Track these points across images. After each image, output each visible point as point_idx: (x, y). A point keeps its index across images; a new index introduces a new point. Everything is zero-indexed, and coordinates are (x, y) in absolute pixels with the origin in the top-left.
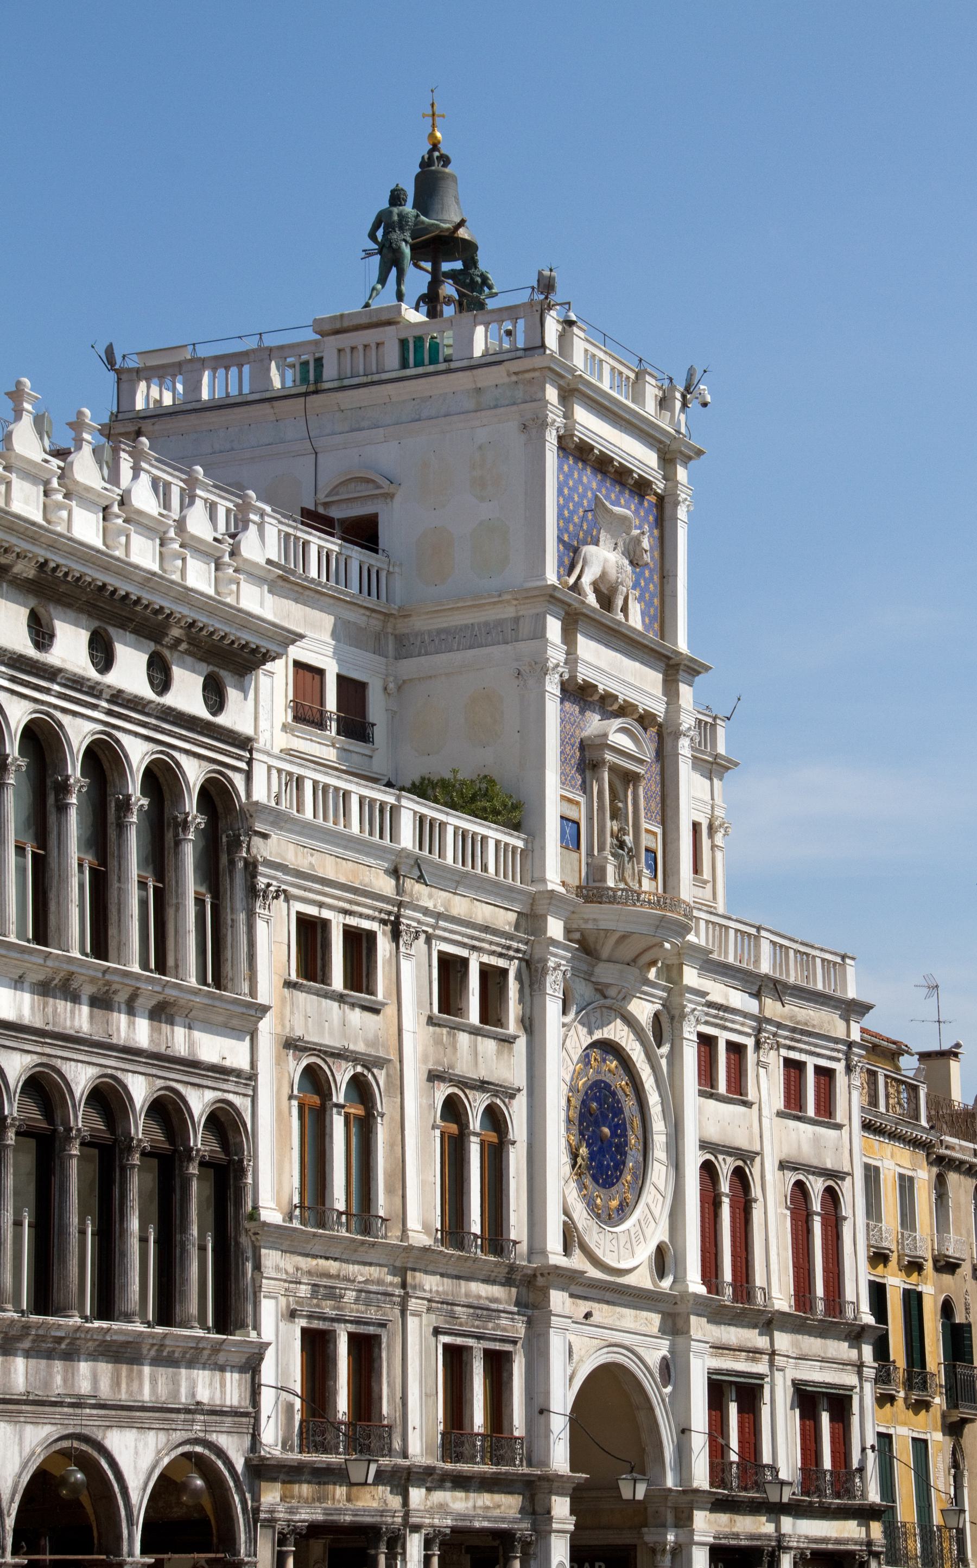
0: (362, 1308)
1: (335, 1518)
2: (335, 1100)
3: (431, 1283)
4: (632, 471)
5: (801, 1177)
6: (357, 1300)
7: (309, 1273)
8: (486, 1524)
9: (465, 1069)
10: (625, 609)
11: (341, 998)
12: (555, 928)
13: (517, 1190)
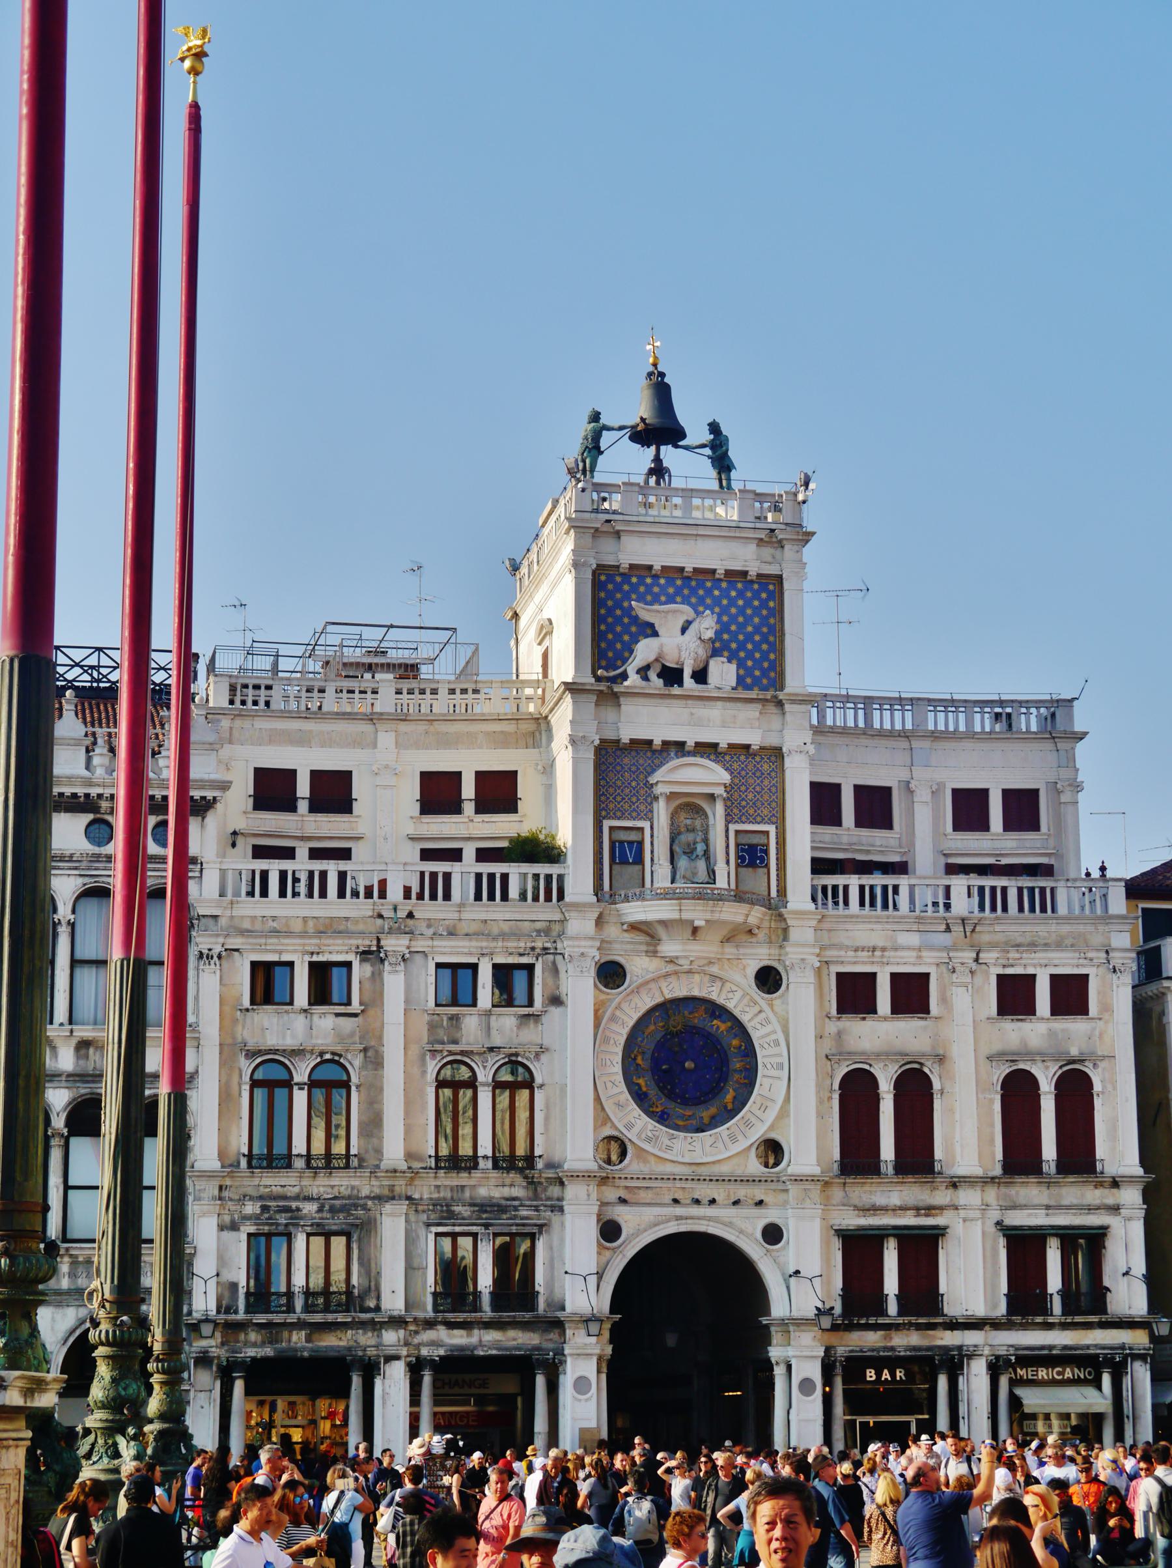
1: (290, 1354)
5: (1021, 1066)
6: (320, 1210)
7: (261, 1198)
8: (494, 1352)
9: (472, 1039)
10: (701, 676)
12: (581, 925)
13: (547, 1119)
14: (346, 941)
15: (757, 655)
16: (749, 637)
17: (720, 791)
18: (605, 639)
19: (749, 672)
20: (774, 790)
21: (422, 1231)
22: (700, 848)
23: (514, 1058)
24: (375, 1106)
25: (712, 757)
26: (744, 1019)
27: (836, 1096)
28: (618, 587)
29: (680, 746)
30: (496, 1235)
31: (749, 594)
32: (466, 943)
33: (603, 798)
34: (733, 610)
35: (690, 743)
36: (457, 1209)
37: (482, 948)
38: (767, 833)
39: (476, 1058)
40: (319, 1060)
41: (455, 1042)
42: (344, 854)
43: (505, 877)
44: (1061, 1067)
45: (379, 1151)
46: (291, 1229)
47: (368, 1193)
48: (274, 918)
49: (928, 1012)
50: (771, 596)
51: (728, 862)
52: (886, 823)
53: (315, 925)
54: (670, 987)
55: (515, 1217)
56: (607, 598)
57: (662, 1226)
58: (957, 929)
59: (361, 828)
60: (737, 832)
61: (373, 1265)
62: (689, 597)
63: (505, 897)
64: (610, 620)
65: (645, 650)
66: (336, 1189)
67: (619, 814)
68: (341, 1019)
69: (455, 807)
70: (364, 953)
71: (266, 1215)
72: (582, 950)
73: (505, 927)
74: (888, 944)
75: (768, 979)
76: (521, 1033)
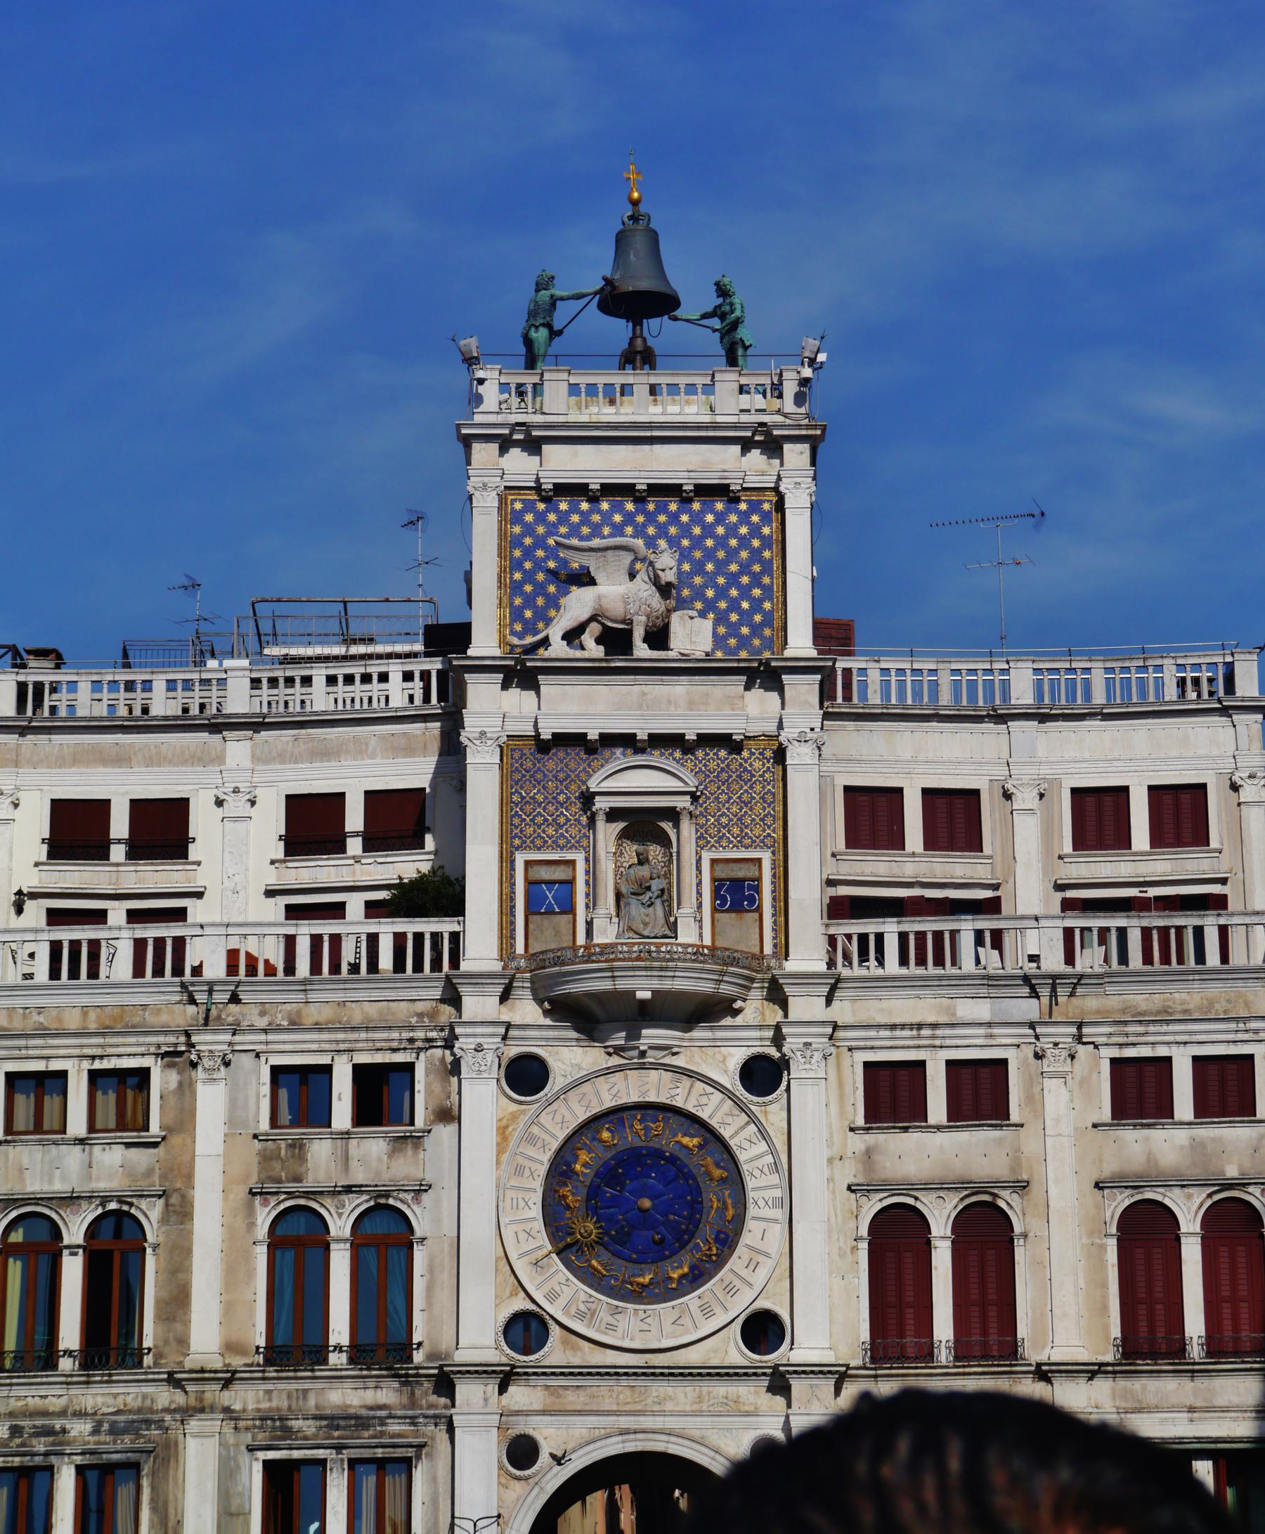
0: (108, 1438)
2: (66, 1242)
3: (246, 1398)
4: (681, 485)
5: (1149, 1195)
6: (96, 1431)
7: (11, 1415)
9: (322, 1176)
10: (658, 637)
11: (81, 1141)
12: (479, 1004)
13: (430, 1289)
14: (142, 1039)
15: (745, 605)
16: (733, 579)
17: (683, 803)
18: (522, 593)
19: (733, 630)
20: (769, 798)
21: (245, 1458)
22: (656, 885)
23: (382, 1201)
24: (180, 1276)
25: (678, 754)
26: (726, 1133)
27: (864, 1245)
28: (541, 518)
29: (627, 741)
30: (352, 1463)
31: (733, 518)
32: (315, 1036)
33: (516, 821)
34: (709, 543)
35: (642, 735)
36: (295, 1424)
37: (337, 1042)
38: (759, 861)
39: (328, 1201)
40: (100, 1211)
41: (298, 1179)
42: (179, 915)
43: (373, 939)
44: (1210, 1195)
45: (183, 1342)
46: (53, 1459)
47: (166, 1405)
48: (40, 1010)
49: (1007, 1116)
50: (766, 518)
51: (700, 906)
52: (973, 842)
53: (98, 1017)
54: (614, 1091)
55: (382, 1434)
56: (523, 535)
57: (598, 1444)
58: (1045, 992)
59: (200, 879)
60: (714, 862)
61: (171, 1511)
62: (644, 526)
63: (373, 966)
64: (528, 565)
65: (578, 605)
66: (120, 1398)
67: (538, 842)
68: (134, 1152)
69: (334, 844)
70: (167, 1054)
71: (18, 1441)
72: (479, 1040)
73: (372, 1010)
74: (943, 1019)
75: (763, 1075)
76: (393, 1164)
